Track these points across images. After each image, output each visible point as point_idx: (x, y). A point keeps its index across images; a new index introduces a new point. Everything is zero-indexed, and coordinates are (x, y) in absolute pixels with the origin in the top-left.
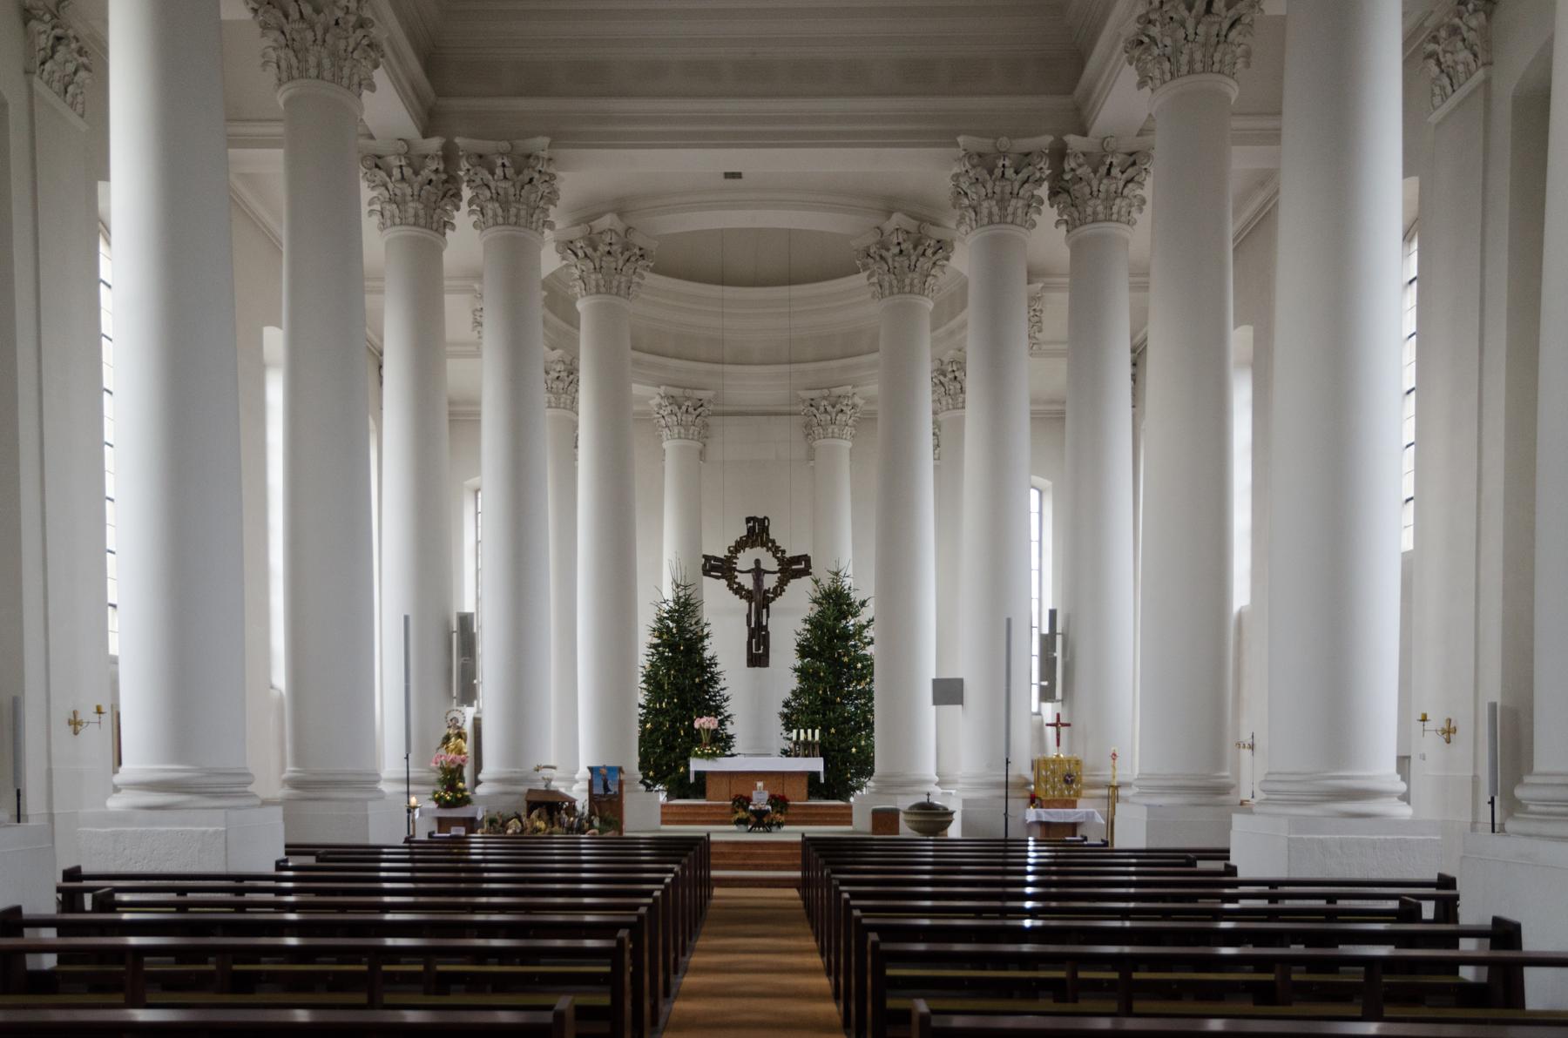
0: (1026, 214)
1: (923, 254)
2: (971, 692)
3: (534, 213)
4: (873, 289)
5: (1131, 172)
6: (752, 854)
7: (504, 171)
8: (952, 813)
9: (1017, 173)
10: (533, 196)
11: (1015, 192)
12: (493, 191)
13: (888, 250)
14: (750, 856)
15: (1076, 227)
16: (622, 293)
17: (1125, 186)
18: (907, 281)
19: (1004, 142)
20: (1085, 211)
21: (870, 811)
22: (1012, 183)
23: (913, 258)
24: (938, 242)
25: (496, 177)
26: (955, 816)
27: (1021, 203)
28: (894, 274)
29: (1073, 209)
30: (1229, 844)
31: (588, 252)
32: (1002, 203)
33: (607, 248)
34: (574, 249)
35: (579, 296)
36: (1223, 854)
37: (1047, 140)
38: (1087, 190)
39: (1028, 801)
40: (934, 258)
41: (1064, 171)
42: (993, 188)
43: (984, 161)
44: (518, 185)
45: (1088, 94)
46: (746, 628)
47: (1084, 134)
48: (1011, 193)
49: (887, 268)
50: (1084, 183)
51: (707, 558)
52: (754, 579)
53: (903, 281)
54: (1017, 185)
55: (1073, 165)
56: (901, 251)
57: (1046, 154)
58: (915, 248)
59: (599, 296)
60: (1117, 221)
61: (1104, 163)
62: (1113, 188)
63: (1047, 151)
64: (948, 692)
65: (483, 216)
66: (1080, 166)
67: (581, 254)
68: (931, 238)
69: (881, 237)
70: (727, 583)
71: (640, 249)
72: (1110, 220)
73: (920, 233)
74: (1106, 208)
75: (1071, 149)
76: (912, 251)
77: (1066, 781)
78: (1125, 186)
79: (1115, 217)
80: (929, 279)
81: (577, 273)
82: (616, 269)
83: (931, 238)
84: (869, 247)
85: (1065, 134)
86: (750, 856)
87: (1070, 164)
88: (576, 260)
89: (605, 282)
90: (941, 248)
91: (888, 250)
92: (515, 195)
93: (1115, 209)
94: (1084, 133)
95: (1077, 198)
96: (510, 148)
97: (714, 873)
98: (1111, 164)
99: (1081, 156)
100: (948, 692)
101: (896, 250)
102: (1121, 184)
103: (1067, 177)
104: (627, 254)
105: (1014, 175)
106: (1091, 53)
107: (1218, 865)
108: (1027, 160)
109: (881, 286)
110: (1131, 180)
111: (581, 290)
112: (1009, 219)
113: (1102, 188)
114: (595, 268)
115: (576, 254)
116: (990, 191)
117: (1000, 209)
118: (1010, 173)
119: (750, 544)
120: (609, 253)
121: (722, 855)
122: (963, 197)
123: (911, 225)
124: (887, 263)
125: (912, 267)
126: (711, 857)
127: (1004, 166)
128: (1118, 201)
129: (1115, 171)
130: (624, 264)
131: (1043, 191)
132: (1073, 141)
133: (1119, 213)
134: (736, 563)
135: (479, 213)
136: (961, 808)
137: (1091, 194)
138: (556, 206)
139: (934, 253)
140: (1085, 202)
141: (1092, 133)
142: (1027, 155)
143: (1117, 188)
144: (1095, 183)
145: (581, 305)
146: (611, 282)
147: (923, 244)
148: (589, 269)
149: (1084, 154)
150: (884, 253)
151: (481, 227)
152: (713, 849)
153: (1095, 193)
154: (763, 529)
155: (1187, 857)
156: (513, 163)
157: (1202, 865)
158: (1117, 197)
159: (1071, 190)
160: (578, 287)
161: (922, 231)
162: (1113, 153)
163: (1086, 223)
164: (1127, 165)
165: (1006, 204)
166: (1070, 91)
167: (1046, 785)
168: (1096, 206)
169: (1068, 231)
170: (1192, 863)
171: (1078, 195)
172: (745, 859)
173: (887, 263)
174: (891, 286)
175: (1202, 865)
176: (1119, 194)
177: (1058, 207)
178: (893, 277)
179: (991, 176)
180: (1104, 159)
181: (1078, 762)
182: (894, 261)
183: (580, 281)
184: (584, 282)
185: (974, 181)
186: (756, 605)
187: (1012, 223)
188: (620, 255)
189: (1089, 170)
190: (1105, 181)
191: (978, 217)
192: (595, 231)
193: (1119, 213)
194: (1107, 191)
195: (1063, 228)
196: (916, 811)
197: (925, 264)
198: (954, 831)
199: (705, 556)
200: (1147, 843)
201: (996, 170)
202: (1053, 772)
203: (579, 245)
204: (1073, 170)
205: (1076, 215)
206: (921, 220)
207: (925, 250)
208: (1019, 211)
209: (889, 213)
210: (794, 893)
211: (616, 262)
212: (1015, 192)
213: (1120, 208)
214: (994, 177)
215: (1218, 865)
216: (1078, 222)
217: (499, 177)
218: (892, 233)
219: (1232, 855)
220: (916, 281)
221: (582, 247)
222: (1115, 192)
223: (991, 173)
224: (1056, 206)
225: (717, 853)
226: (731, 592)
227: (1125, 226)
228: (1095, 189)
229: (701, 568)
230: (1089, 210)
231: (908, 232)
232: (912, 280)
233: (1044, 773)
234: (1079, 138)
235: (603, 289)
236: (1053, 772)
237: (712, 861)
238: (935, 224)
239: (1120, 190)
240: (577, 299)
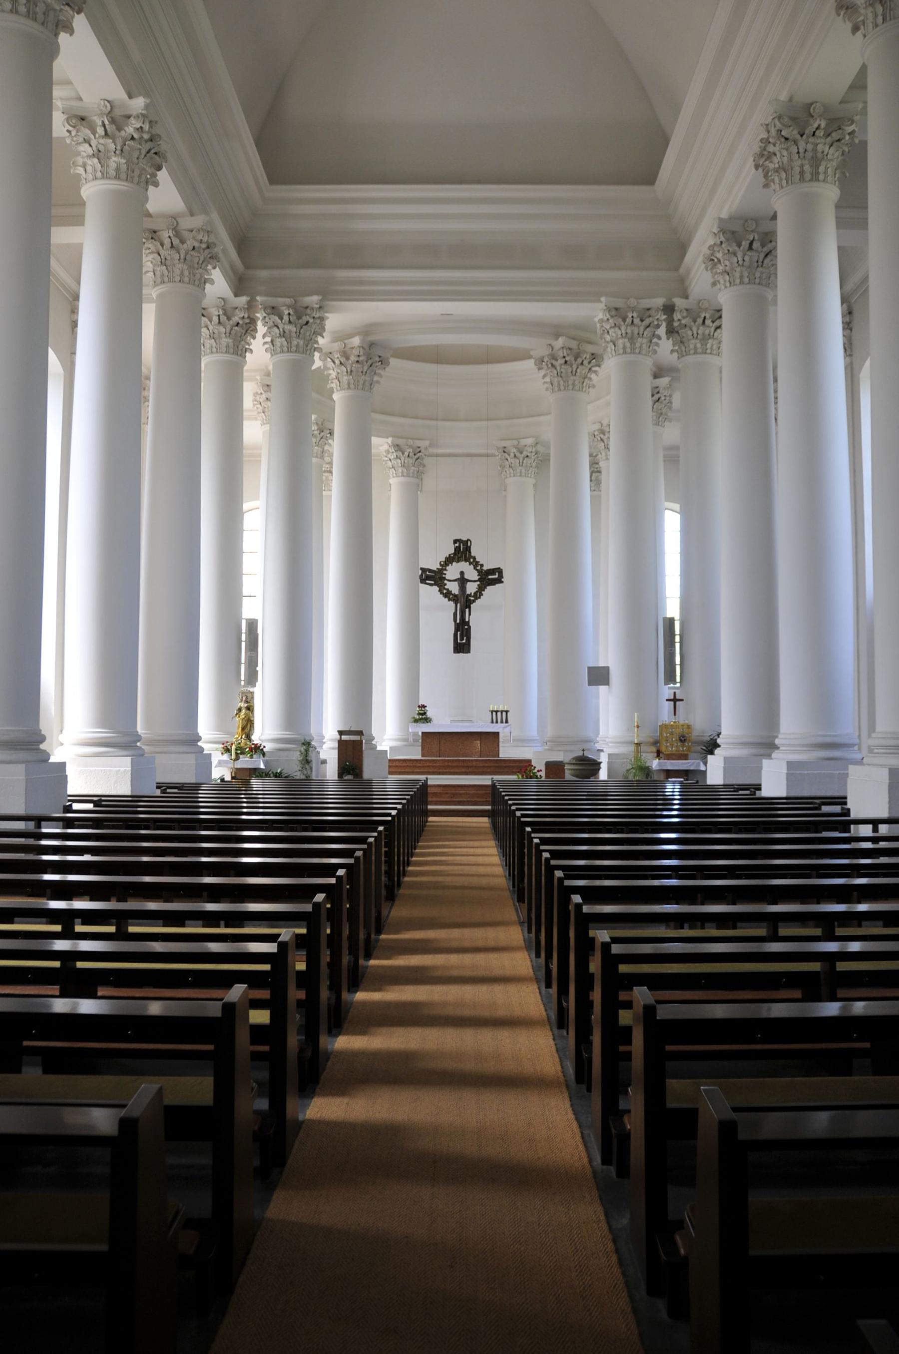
0: (649, 347)
1: (582, 364)
2: (615, 676)
3: (309, 343)
4: (546, 385)
5: (717, 323)
6: (456, 794)
7: (289, 318)
8: (600, 763)
9: (642, 321)
10: (308, 334)
11: (641, 333)
12: (281, 330)
13: (557, 360)
14: (454, 795)
15: (683, 356)
16: (366, 388)
17: (715, 331)
18: (570, 382)
19: (633, 302)
20: (689, 346)
21: (544, 763)
22: (639, 327)
23: (575, 367)
24: (593, 354)
25: (283, 321)
26: (602, 765)
27: (645, 341)
28: (561, 376)
29: (681, 345)
30: (846, 792)
31: (342, 361)
32: (632, 340)
33: (356, 359)
34: (332, 358)
35: (335, 390)
36: (841, 800)
37: (660, 302)
38: (690, 333)
39: (655, 755)
40: (590, 366)
41: (673, 320)
42: (626, 330)
43: (617, 312)
44: (299, 326)
45: (688, 271)
46: (453, 623)
47: (687, 298)
48: (638, 334)
49: (556, 372)
50: (687, 329)
51: (423, 570)
52: (459, 586)
53: (568, 382)
54: (642, 329)
55: (679, 317)
56: (566, 362)
57: (660, 309)
58: (576, 360)
59: (350, 391)
60: (711, 353)
61: (700, 317)
62: (707, 332)
63: (662, 308)
64: (599, 676)
65: (273, 346)
66: (684, 318)
67: (337, 362)
68: (587, 353)
69: (552, 350)
70: (438, 589)
71: (380, 357)
72: (706, 353)
73: (579, 349)
74: (702, 345)
75: (678, 307)
76: (574, 362)
77: (681, 741)
78: (715, 331)
79: (709, 351)
80: (586, 380)
81: (333, 374)
82: (362, 372)
83: (587, 353)
84: (544, 357)
85: (674, 298)
86: (454, 795)
87: (677, 316)
88: (334, 366)
89: (354, 381)
90: (594, 358)
91: (557, 360)
92: (296, 333)
93: (709, 346)
94: (687, 298)
95: (683, 337)
96: (294, 302)
97: (430, 807)
98: (705, 318)
99: (685, 311)
100: (599, 676)
101: (563, 361)
102: (712, 330)
103: (676, 324)
104: (370, 362)
105: (640, 323)
106: (690, 245)
107: (837, 809)
108: (648, 313)
109: (552, 385)
110: (719, 327)
111: (337, 386)
112: (637, 351)
113: (700, 332)
114: (347, 372)
115: (334, 362)
116: (624, 332)
117: (631, 344)
118: (637, 321)
119: (456, 560)
120: (358, 362)
121: (435, 794)
122: (606, 334)
123: (574, 344)
124: (556, 369)
125: (574, 372)
126: (429, 796)
127: (632, 317)
128: (710, 341)
129: (708, 322)
130: (368, 369)
131: (662, 331)
132: (679, 302)
133: (711, 348)
134: (445, 574)
135: (270, 344)
136: (607, 760)
137: (693, 335)
138: (323, 337)
139: (589, 363)
140: (689, 340)
141: (691, 297)
142: (649, 309)
143: (710, 332)
144: (695, 329)
145: (336, 396)
146: (358, 381)
147: (581, 357)
148: (342, 372)
149: (687, 310)
150: (554, 362)
151: (271, 353)
152: (430, 790)
153: (695, 335)
154: (466, 548)
155: (813, 803)
156: (296, 311)
157: (825, 809)
158: (710, 338)
159: (680, 332)
160: (334, 385)
161: (581, 348)
162: (706, 310)
163: (690, 354)
164: (715, 318)
165: (635, 341)
166: (677, 269)
167: (666, 743)
168: (695, 344)
169: (678, 357)
170: (819, 808)
171: (685, 335)
172: (451, 798)
173: (556, 369)
174: (559, 385)
175: (825, 809)
176: (711, 337)
177: (673, 340)
178: (560, 379)
179: (624, 322)
180: (700, 314)
181: (689, 727)
182: (561, 368)
183: (337, 381)
184: (339, 381)
185: (613, 325)
186: (461, 606)
187: (639, 353)
188: (365, 363)
189: (691, 320)
190: (701, 328)
191: (617, 347)
192: (348, 346)
193: (711, 348)
194: (703, 334)
195: (675, 355)
196: (574, 762)
197: (583, 370)
198: (603, 775)
199: (422, 569)
200: (787, 792)
201: (627, 320)
202: (672, 734)
203: (336, 356)
204: (679, 320)
205: (683, 348)
206: (581, 341)
207: (583, 361)
208: (644, 346)
209: (557, 336)
210: (486, 819)
211: (363, 367)
212: (641, 333)
213: (712, 345)
214: (626, 323)
215: (837, 809)
216: (684, 354)
217: (285, 321)
218: (560, 349)
219: (849, 801)
220: (577, 382)
221: (338, 358)
222: (709, 335)
223: (624, 320)
224: (671, 339)
225: (431, 793)
226: (442, 596)
227: (716, 357)
228: (695, 332)
229: (418, 577)
230: (692, 346)
231: (570, 349)
232: (574, 381)
233: (665, 735)
234: (683, 300)
235: (352, 386)
236: (672, 734)
237: (429, 799)
238: (590, 342)
239: (712, 334)
240: (333, 392)
